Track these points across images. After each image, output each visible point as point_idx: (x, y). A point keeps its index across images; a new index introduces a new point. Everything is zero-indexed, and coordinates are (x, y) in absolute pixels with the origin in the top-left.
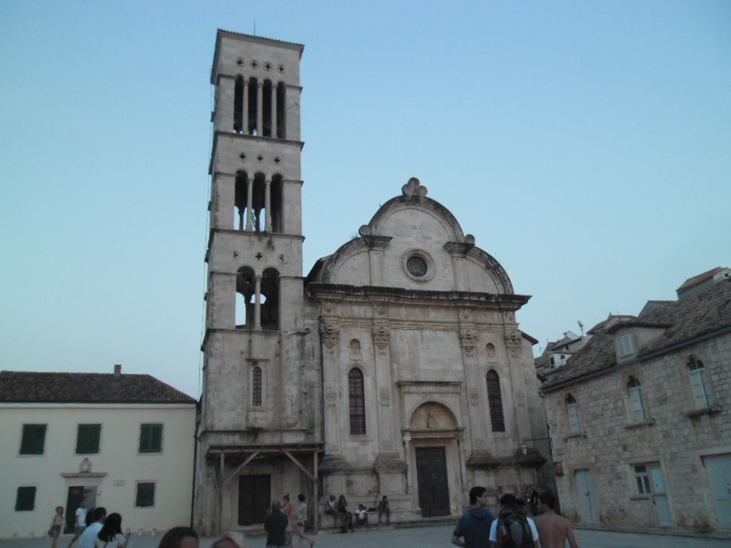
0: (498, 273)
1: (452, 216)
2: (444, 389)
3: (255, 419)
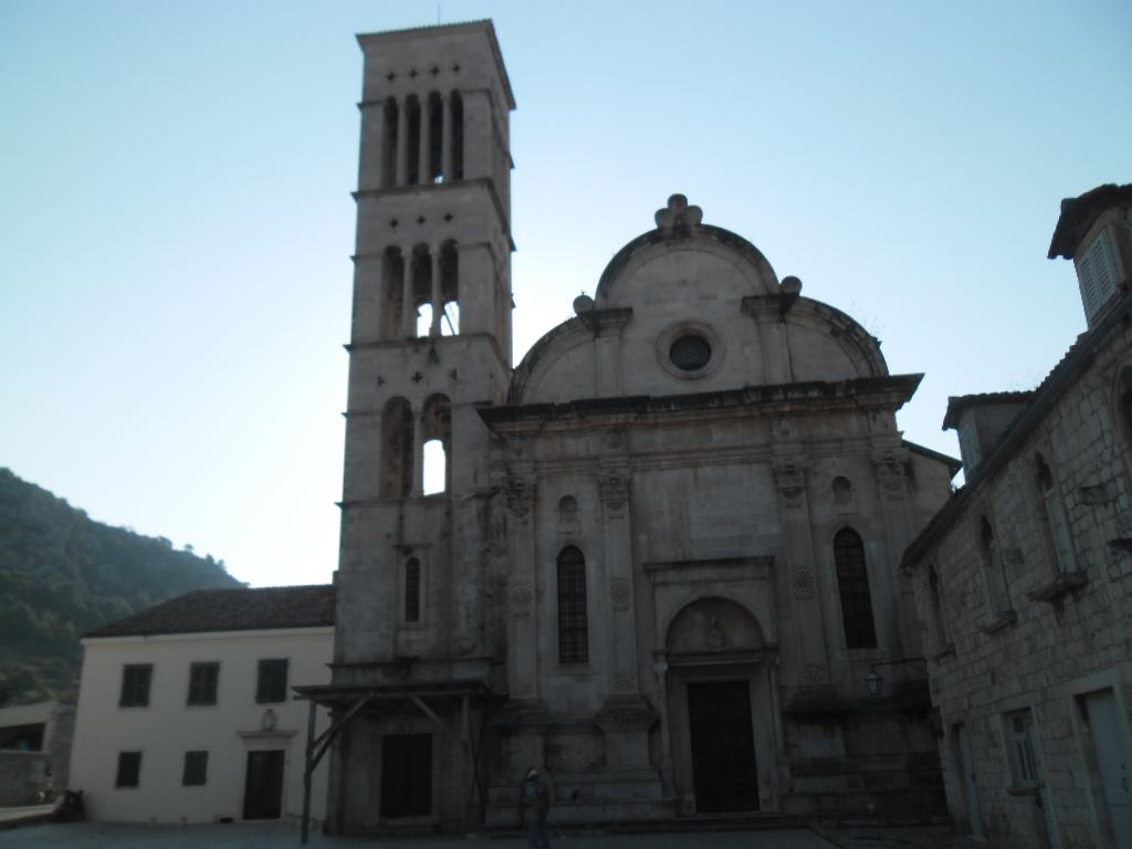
2: (735, 572)
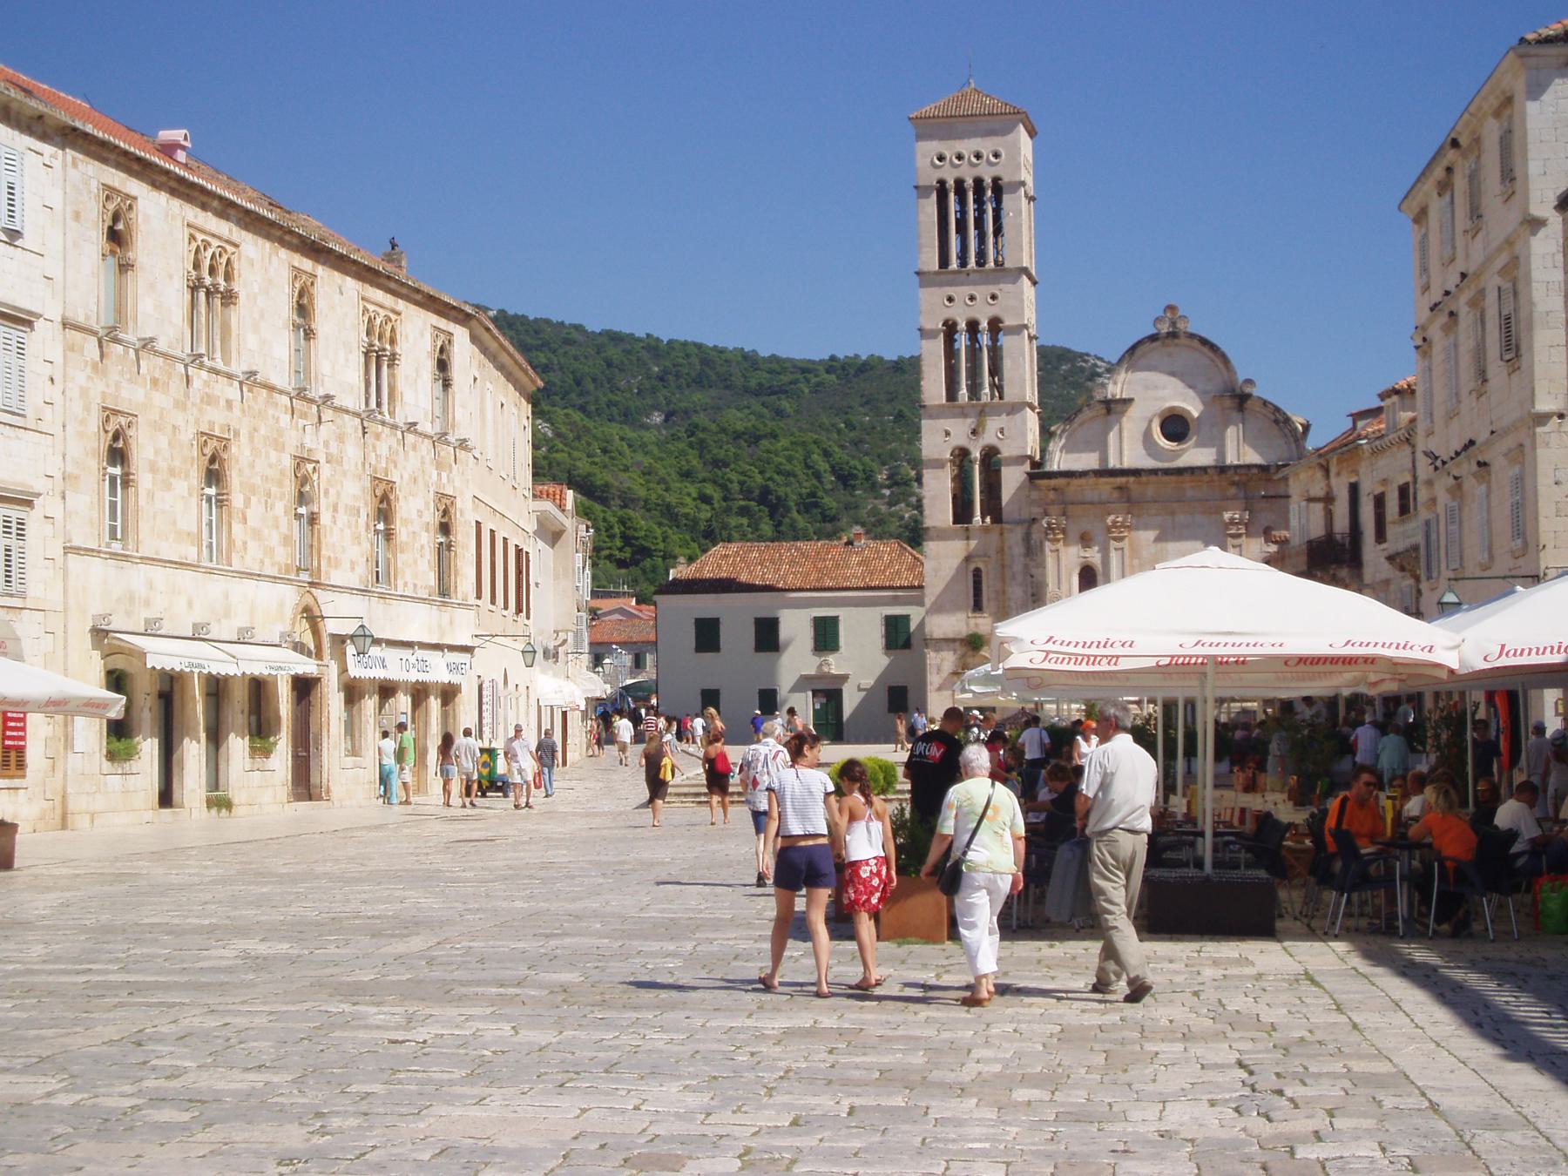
3: (976, 625)
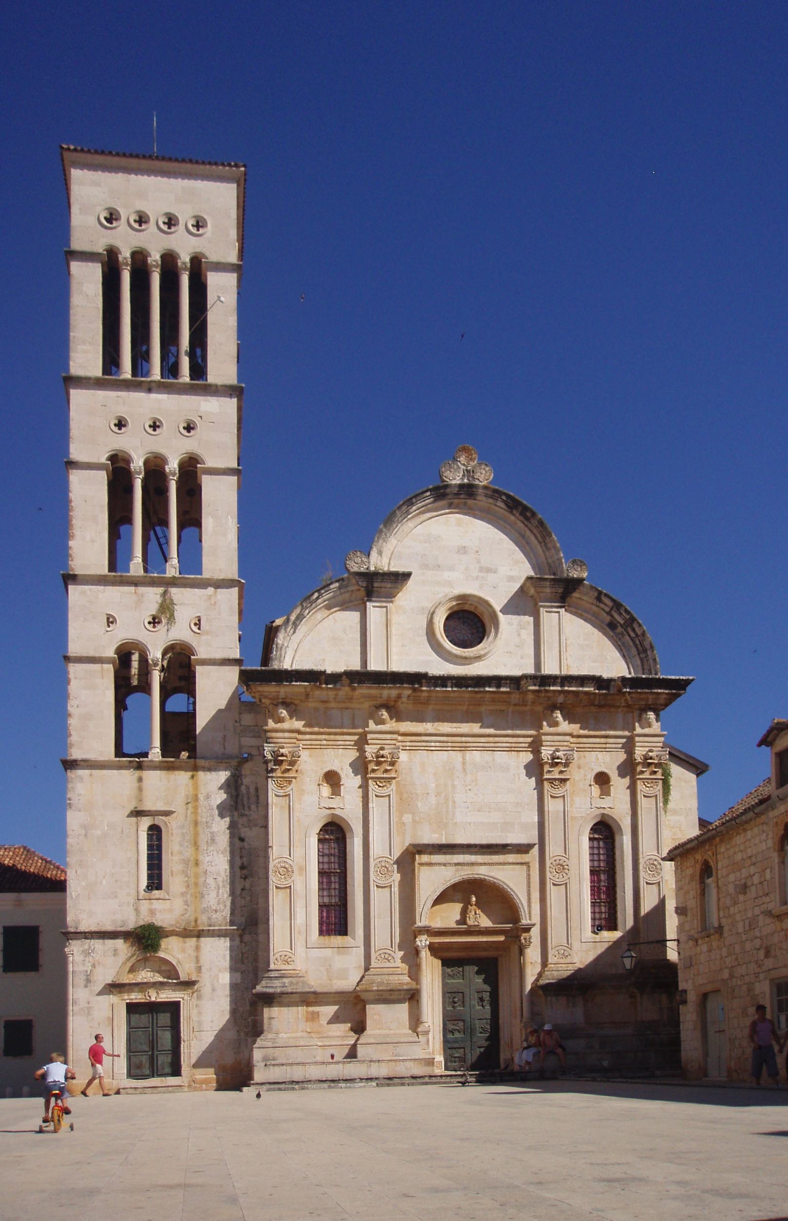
0: (633, 635)
1: (541, 523)
3: (152, 912)
